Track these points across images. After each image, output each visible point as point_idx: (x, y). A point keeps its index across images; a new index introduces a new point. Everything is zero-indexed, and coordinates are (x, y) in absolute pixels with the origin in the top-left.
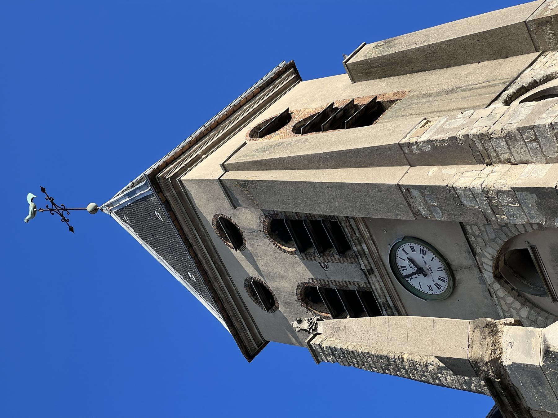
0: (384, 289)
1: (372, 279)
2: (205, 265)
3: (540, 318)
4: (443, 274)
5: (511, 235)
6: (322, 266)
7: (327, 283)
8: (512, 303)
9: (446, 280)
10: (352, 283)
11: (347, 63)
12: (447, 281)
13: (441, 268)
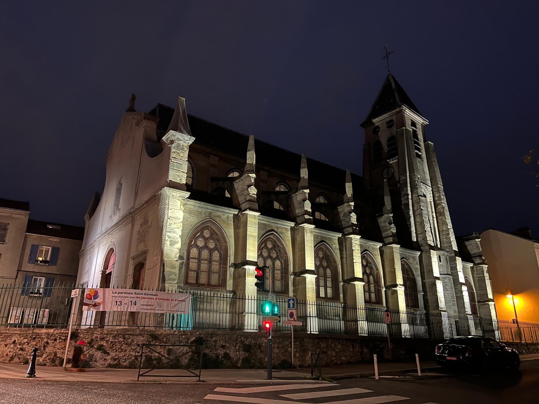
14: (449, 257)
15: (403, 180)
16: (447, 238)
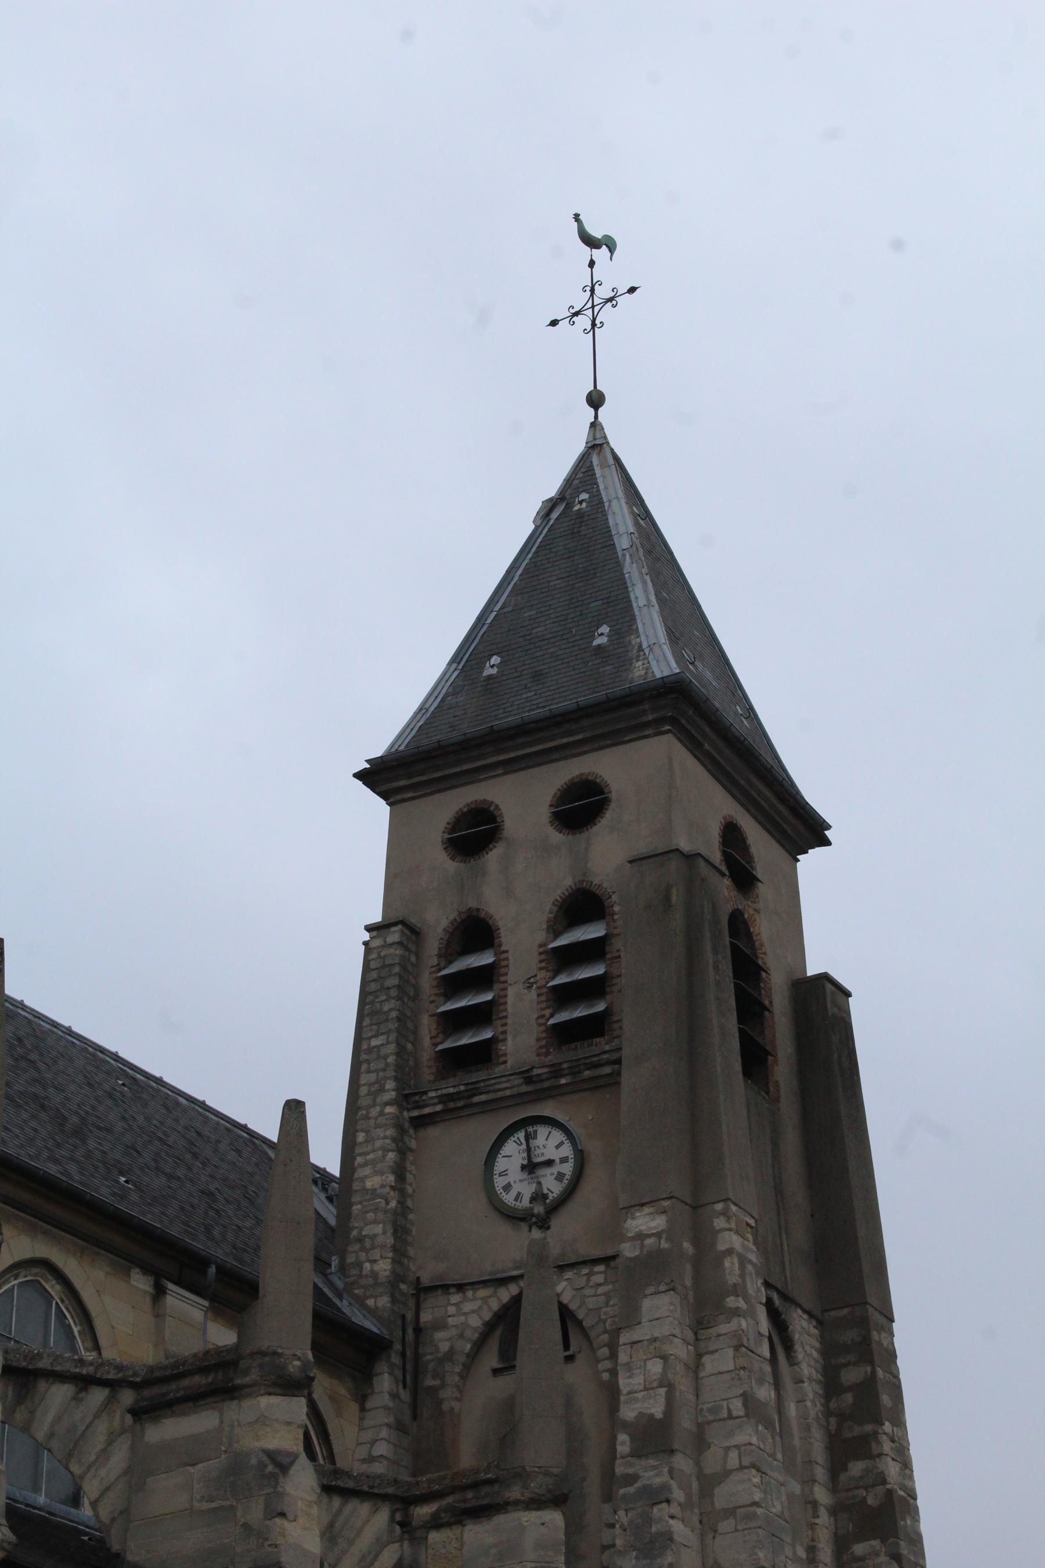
0: (500, 1094)
1: (517, 1081)
3: (469, 1346)
5: (592, 1334)
6: (530, 978)
7: (502, 979)
9: (518, 1203)
12: (516, 1207)
15: (641, 1236)
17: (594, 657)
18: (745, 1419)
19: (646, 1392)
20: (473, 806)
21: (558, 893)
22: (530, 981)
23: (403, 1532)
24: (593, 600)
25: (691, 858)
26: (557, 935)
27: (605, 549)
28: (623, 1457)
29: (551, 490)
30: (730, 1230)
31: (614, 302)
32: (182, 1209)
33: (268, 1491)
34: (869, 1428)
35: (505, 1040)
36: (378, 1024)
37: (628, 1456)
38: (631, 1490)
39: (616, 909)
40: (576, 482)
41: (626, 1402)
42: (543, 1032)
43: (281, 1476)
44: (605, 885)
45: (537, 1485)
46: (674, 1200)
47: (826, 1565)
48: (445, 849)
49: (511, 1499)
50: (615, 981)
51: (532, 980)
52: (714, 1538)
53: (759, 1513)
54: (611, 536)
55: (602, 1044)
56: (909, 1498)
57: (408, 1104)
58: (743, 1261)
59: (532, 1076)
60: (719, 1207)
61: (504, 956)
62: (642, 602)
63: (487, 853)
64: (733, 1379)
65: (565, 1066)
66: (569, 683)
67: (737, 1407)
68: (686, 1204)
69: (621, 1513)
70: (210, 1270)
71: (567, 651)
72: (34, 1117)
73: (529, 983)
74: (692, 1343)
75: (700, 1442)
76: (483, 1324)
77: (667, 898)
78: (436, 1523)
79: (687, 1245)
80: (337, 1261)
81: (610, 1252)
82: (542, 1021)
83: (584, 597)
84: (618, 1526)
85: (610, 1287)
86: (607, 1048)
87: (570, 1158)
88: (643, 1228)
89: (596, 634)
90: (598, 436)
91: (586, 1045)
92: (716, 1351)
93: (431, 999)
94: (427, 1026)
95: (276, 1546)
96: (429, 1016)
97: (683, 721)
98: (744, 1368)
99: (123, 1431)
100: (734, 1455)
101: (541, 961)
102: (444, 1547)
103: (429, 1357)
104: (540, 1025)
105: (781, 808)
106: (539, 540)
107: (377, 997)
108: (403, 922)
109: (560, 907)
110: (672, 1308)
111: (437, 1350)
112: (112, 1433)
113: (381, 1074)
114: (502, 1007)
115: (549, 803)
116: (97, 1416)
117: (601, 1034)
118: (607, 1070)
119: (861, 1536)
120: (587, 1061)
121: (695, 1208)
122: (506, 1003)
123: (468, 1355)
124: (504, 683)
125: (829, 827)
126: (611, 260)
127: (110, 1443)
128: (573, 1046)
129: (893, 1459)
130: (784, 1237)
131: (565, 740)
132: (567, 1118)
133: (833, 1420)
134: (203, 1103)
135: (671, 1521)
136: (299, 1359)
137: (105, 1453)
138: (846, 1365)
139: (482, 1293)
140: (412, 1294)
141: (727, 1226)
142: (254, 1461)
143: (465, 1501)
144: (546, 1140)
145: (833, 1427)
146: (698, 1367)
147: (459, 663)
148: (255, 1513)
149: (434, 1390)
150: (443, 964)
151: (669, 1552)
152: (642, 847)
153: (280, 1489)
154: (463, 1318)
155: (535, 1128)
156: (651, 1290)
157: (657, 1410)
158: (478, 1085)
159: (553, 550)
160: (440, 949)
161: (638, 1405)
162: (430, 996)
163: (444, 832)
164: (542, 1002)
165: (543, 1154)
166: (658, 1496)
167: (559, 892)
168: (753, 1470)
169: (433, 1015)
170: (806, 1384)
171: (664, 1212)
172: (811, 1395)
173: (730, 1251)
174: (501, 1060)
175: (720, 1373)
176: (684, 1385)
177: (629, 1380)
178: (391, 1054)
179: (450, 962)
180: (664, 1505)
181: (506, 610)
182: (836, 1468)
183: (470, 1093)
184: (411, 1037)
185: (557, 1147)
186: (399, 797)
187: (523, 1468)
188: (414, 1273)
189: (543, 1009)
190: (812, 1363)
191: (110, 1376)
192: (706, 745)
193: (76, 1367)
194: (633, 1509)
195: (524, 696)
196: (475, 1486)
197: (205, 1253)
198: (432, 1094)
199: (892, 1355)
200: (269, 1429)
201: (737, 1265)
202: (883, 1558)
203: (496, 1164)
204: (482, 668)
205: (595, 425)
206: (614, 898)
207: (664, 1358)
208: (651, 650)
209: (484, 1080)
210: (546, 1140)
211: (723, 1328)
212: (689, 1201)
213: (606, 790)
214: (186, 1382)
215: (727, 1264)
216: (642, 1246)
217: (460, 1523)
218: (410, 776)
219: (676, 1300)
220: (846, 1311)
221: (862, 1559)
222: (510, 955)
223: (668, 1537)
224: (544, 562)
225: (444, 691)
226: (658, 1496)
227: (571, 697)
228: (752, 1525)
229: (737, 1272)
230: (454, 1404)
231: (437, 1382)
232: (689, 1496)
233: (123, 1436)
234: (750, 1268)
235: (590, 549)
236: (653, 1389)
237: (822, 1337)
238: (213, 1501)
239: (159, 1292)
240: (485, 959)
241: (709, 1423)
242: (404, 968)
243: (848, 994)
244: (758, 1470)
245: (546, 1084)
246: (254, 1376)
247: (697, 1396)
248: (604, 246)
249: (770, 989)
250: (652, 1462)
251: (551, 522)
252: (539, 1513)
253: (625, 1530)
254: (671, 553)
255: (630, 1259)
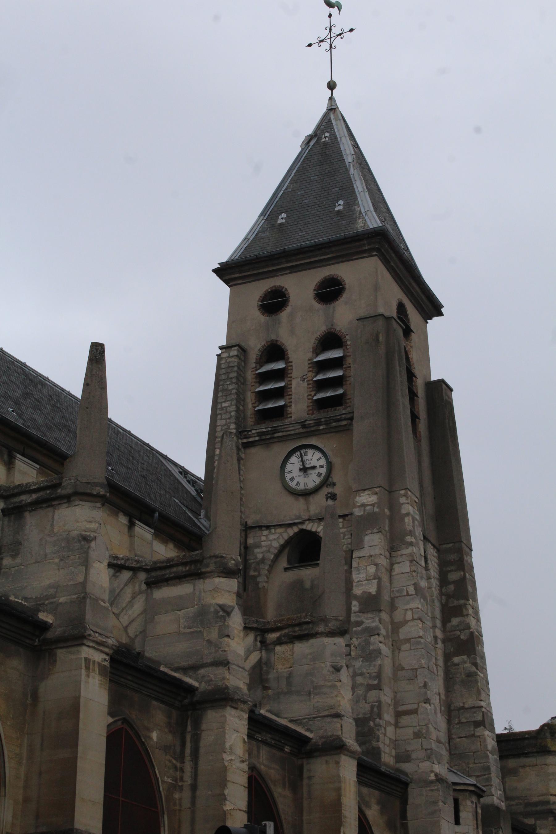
0: (289, 433)
2: (301, 256)
3: (272, 556)
4: (302, 487)
6: (303, 376)
7: (289, 375)
8: (283, 538)
9: (297, 487)
10: (290, 400)
11: (442, 383)
12: (297, 489)
13: (307, 486)
14: (483, 808)
15: (364, 505)
16: (473, 735)
17: (336, 216)
18: (415, 596)
19: (366, 582)
20: (274, 288)
21: (318, 334)
22: (304, 377)
23: (262, 646)
24: (334, 187)
25: (388, 319)
26: (317, 355)
27: (339, 162)
28: (355, 613)
29: (310, 130)
30: (408, 503)
31: (342, 36)
32: (136, 484)
33: (220, 624)
34: (462, 602)
35: (290, 406)
36: (226, 396)
37: (358, 612)
38: (359, 628)
39: (349, 343)
40: (322, 127)
41: (356, 586)
42: (311, 403)
43: (227, 617)
44: (343, 331)
45: (333, 625)
46: (381, 488)
47: (441, 667)
48: (259, 309)
49: (319, 632)
50: (348, 379)
51: (305, 377)
52: (399, 653)
53: (422, 641)
54: (342, 155)
55: (341, 411)
56: (479, 636)
57: (241, 436)
58: (414, 519)
59: (305, 425)
60: (402, 492)
61: (290, 364)
62: (360, 189)
63: (281, 313)
64: (409, 576)
65: (323, 420)
66: (324, 229)
67: (412, 590)
68: (386, 490)
69: (354, 640)
70: (156, 515)
71: (321, 212)
72: (67, 435)
73: (303, 378)
74: (388, 558)
75: (393, 607)
76: (280, 546)
77: (377, 339)
78: (279, 642)
79: (386, 510)
80: (204, 512)
81: (346, 512)
82: (310, 397)
83: (329, 186)
84: (352, 646)
85: (345, 530)
86: (344, 412)
87: (324, 465)
88: (365, 501)
89: (337, 204)
90: (333, 104)
91: (333, 410)
92: (401, 562)
93: (252, 384)
94: (250, 398)
95: (225, 651)
96: (251, 393)
97: (383, 250)
98: (415, 571)
99: (140, 592)
100: (409, 613)
101: (309, 368)
102: (284, 654)
103: (252, 561)
104: (309, 399)
105: (423, 297)
106: (304, 156)
107: (226, 382)
108: (238, 345)
109: (319, 341)
110: (380, 541)
111: (256, 558)
112: (134, 593)
113: (228, 421)
114: (289, 390)
115: (313, 288)
116: (126, 585)
117: (341, 405)
118: (344, 423)
119: (457, 654)
120: (335, 418)
121: (390, 492)
122: (291, 388)
123: (272, 561)
124: (289, 227)
125: (443, 307)
126: (339, 14)
127: (133, 598)
128: (326, 410)
129: (473, 617)
130: (424, 507)
131: (322, 258)
132: (323, 446)
133: (444, 597)
134: (129, 432)
135: (380, 644)
136: (234, 560)
137: (130, 603)
138: (450, 571)
139: (279, 530)
140: (243, 530)
141: (407, 502)
142: (212, 609)
143: (294, 632)
144: (312, 456)
145: (444, 601)
146: (391, 570)
147: (265, 216)
148: (214, 634)
149: (254, 577)
150: (258, 367)
151: (379, 659)
152: (363, 313)
153: (226, 624)
154: (269, 542)
155: (306, 450)
156: (369, 532)
157: (373, 590)
158: (278, 428)
159: (312, 161)
160: (256, 359)
161: (363, 587)
162: (251, 383)
163: (258, 301)
164: (310, 388)
165: (310, 463)
166: (372, 632)
167: (319, 333)
168: (419, 621)
169: (253, 393)
170: (432, 580)
171: (376, 494)
172: (434, 585)
173: (408, 514)
174: (289, 416)
175: (402, 573)
176: (385, 579)
177: (358, 575)
178: (234, 411)
179: (261, 366)
180: (376, 636)
181: (288, 190)
182: (445, 621)
183: (273, 432)
184: (242, 403)
185: (318, 460)
186: (235, 283)
187: (325, 617)
188: (244, 519)
189: (311, 391)
190: (435, 570)
191: (133, 565)
192: (392, 263)
193: (114, 560)
194: (361, 638)
195: (300, 234)
196: (300, 624)
197: (154, 506)
198: (254, 432)
199: (472, 567)
200: (219, 594)
201: (411, 521)
202: (468, 665)
203: (286, 467)
204: (277, 219)
205: (331, 99)
206: (347, 337)
207: (376, 565)
208: (366, 214)
209: (281, 426)
210: (312, 456)
211: (404, 552)
212: (387, 488)
213: (343, 283)
214: (174, 569)
215: (407, 520)
216: (364, 510)
217: (292, 642)
218: (241, 272)
219: (382, 537)
220: (451, 545)
221: (458, 665)
222: (293, 364)
223: (379, 652)
224: (307, 167)
225: (257, 230)
226: (372, 632)
227: (325, 236)
228: (418, 647)
229: (411, 524)
230: (265, 584)
231: (256, 573)
232: (387, 631)
233: (140, 595)
234: (416, 523)
235: (332, 161)
236: (370, 580)
237: (439, 558)
238: (191, 629)
239: (131, 525)
240: (280, 365)
241: (397, 597)
242: (239, 368)
243: (451, 390)
244: (421, 621)
245: (313, 429)
246: (212, 567)
247: (391, 584)
248: (336, 7)
249: (417, 386)
250: (370, 615)
251: (310, 147)
252: (333, 639)
253: (356, 648)
254: (368, 166)
255: (358, 516)
